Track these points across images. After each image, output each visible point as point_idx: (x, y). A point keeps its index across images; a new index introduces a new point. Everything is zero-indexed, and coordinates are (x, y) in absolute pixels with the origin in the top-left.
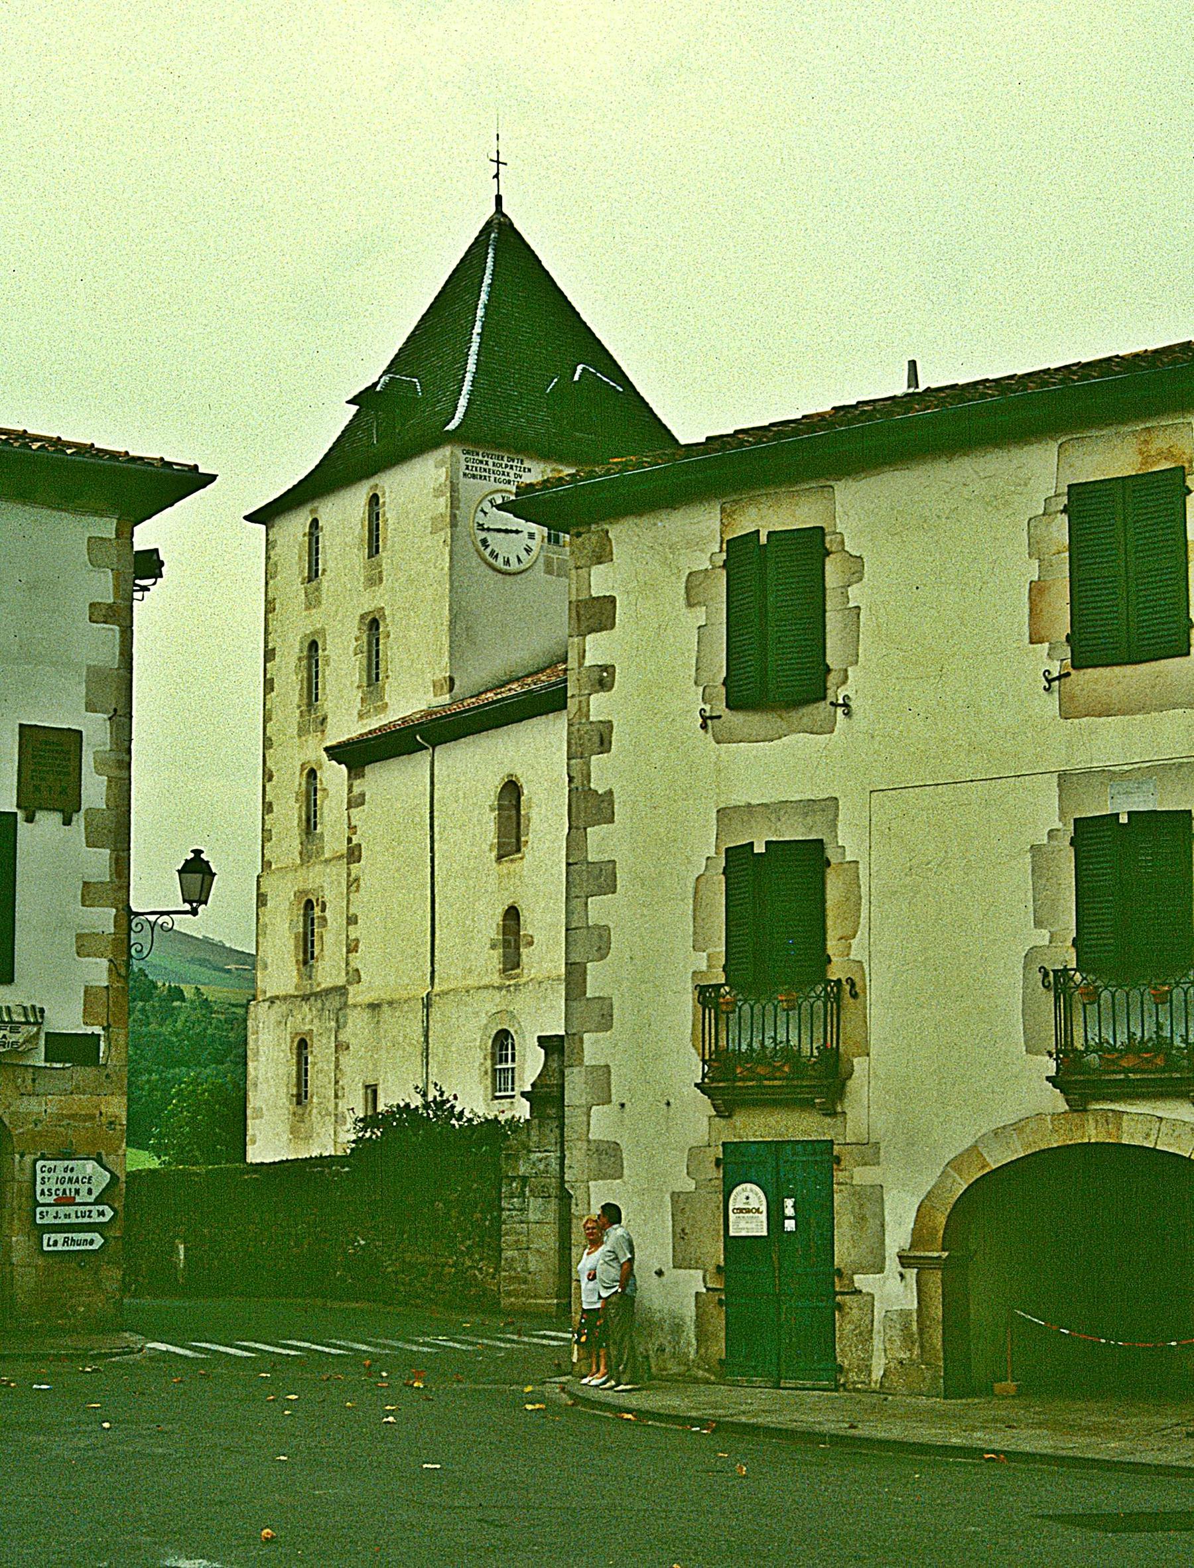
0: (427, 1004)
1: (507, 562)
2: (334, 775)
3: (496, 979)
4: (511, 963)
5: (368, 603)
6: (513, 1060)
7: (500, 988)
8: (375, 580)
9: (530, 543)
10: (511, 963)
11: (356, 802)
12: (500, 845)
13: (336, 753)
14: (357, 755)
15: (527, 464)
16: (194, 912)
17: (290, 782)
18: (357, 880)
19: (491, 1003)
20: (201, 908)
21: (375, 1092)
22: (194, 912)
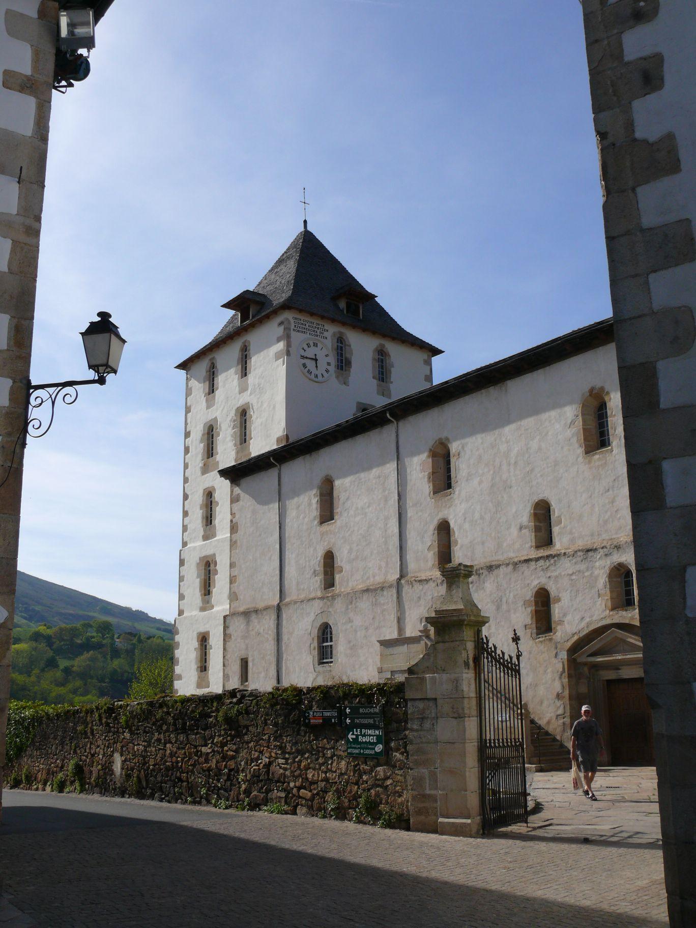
0: (279, 608)
1: (316, 376)
2: (223, 487)
3: (319, 594)
4: (329, 583)
5: (241, 401)
6: (331, 641)
7: (322, 598)
8: (243, 389)
9: (329, 367)
10: (329, 583)
11: (234, 500)
12: (321, 516)
13: (224, 473)
14: (235, 474)
15: (326, 328)
16: (101, 381)
17: (197, 498)
18: (236, 542)
19: (317, 604)
20: (110, 378)
21: (247, 662)
22: (101, 381)
